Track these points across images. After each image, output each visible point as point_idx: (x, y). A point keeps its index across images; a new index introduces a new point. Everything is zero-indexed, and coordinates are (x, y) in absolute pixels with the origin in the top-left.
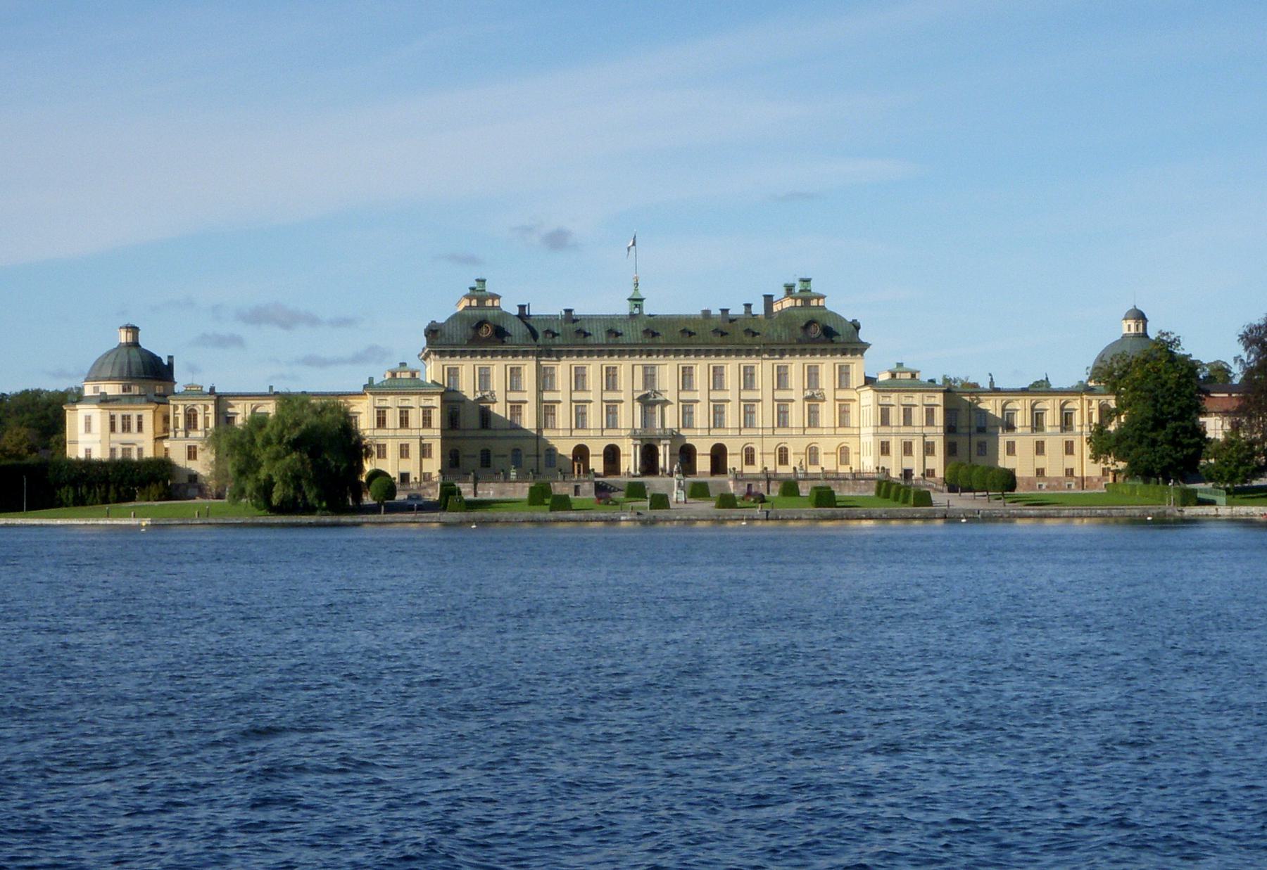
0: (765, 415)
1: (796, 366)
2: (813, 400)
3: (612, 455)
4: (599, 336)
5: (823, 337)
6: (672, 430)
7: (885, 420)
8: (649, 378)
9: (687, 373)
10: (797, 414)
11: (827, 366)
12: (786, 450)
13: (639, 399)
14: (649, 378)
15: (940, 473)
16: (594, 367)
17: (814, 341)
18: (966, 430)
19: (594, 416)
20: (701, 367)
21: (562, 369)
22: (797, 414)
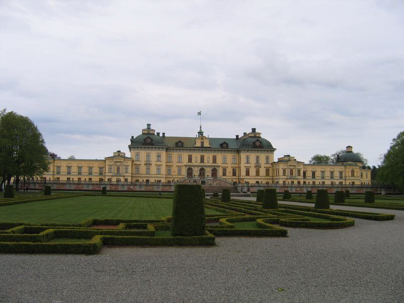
10: (253, 172)
11: (263, 156)
22: (253, 172)
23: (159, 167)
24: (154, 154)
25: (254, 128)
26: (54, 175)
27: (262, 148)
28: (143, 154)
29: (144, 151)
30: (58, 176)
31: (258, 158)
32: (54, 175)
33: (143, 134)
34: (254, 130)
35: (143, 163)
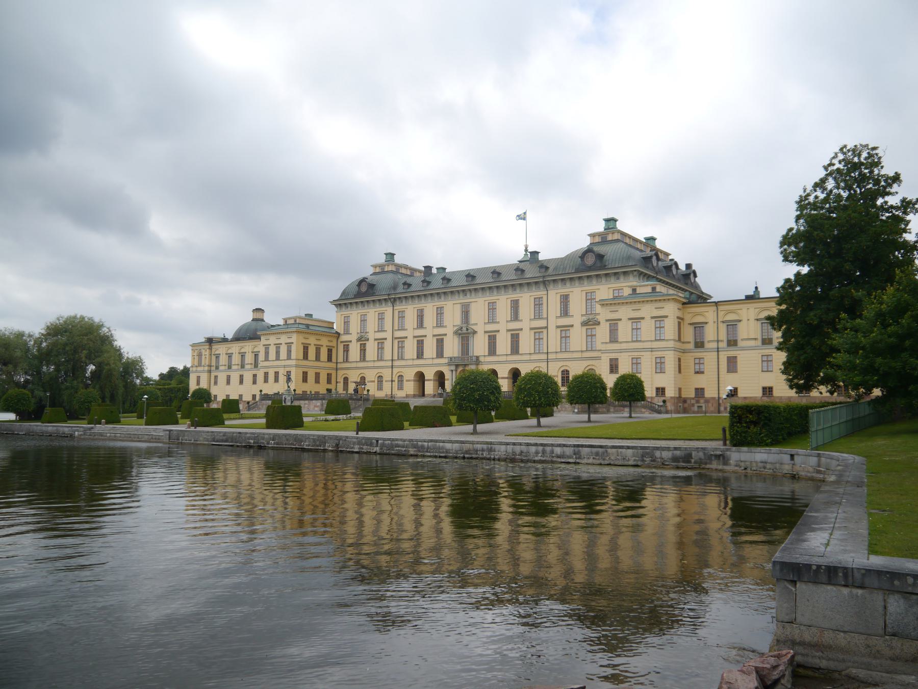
0: (553, 340)
1: (577, 294)
2: (590, 323)
3: (440, 378)
4: (437, 283)
5: (599, 264)
6: (477, 357)
7: (613, 339)
8: (466, 314)
9: (492, 308)
10: (578, 338)
11: (604, 290)
12: (567, 371)
13: (456, 333)
14: (466, 314)
15: (670, 393)
16: (430, 308)
17: (590, 269)
18: (714, 345)
19: (430, 348)
20: (503, 301)
21: (410, 310)
22: (578, 338)
23: (381, 342)
24: (372, 313)
25: (610, 216)
26: (210, 372)
27: (604, 267)
28: (355, 315)
29: (356, 312)
30: (216, 374)
31: (590, 299)
32: (210, 372)
33: (375, 274)
34: (611, 222)
35: (353, 337)
